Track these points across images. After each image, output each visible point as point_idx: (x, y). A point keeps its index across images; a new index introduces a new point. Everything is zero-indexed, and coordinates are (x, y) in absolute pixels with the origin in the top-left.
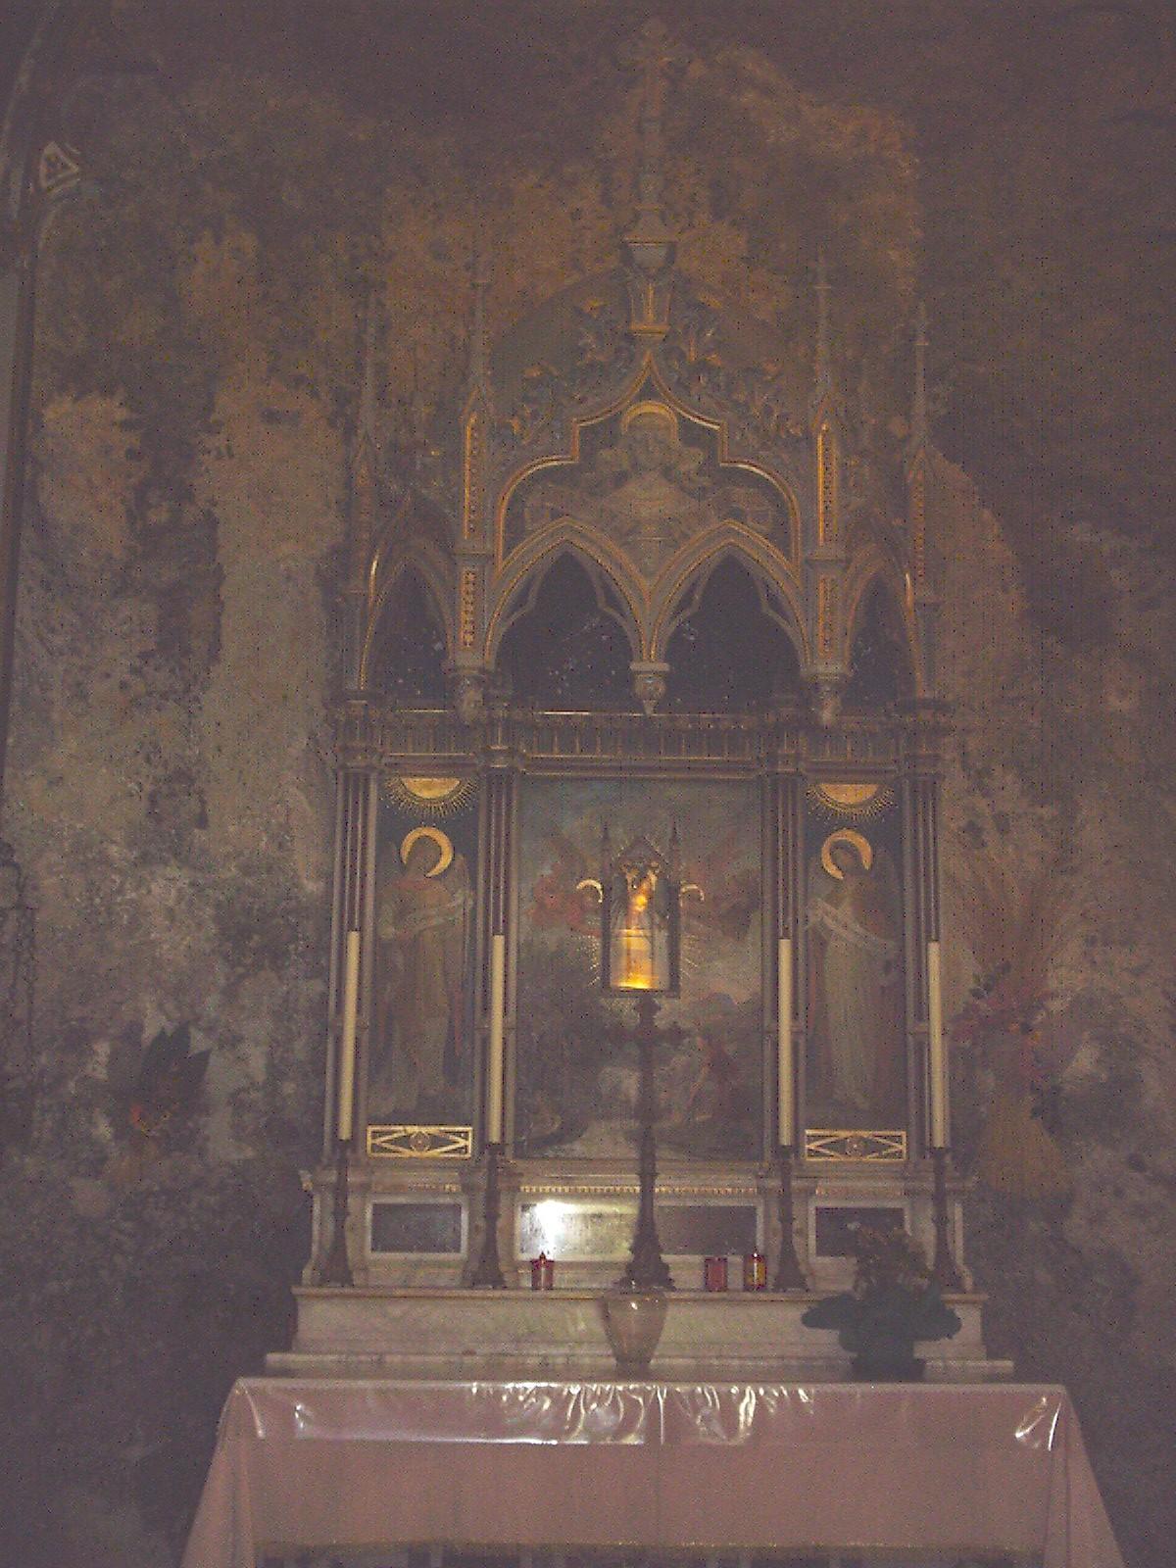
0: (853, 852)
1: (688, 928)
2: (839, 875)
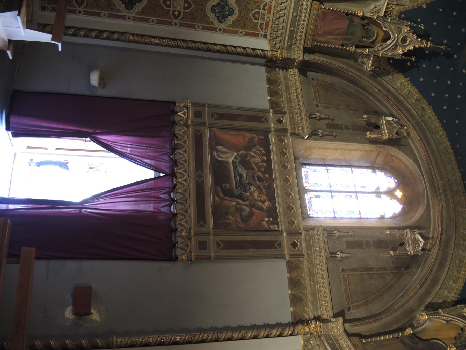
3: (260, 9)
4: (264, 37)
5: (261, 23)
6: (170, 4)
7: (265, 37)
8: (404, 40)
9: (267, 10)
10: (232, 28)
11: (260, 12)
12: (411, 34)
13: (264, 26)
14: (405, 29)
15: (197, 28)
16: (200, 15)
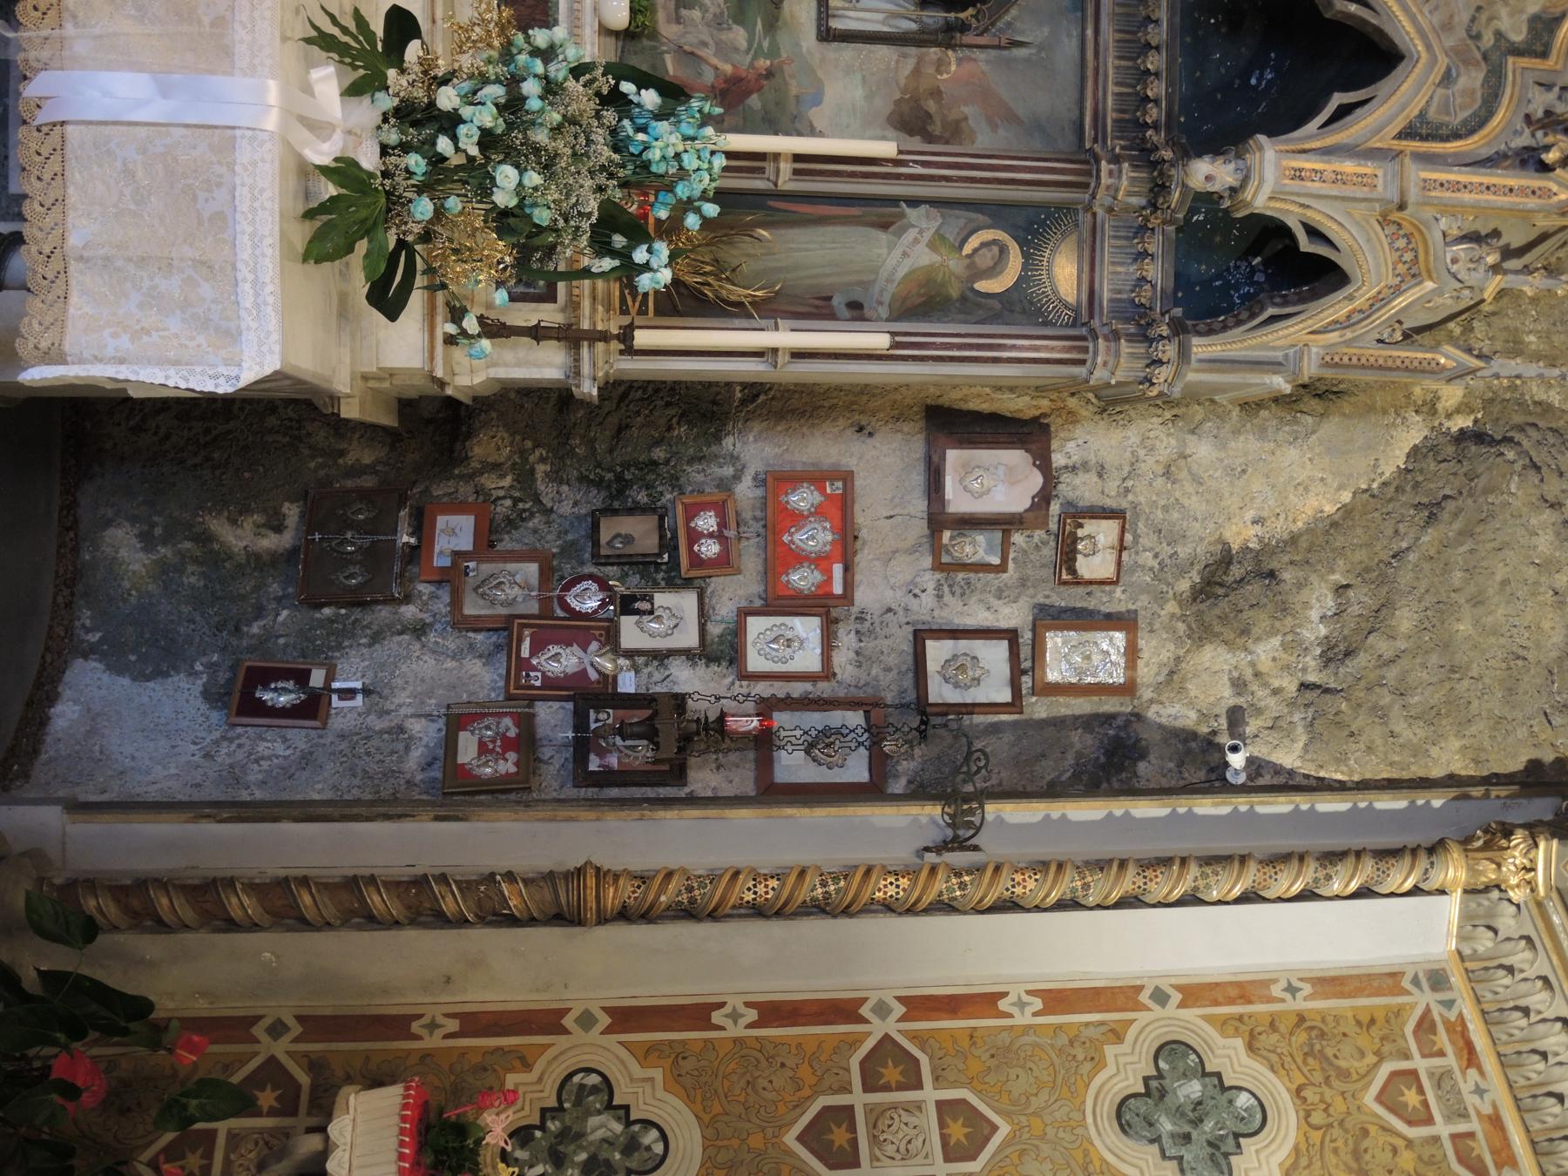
0: (993, 271)
1: (905, 56)
2: (967, 249)
3: (1407, 1056)
9: (1449, 1049)
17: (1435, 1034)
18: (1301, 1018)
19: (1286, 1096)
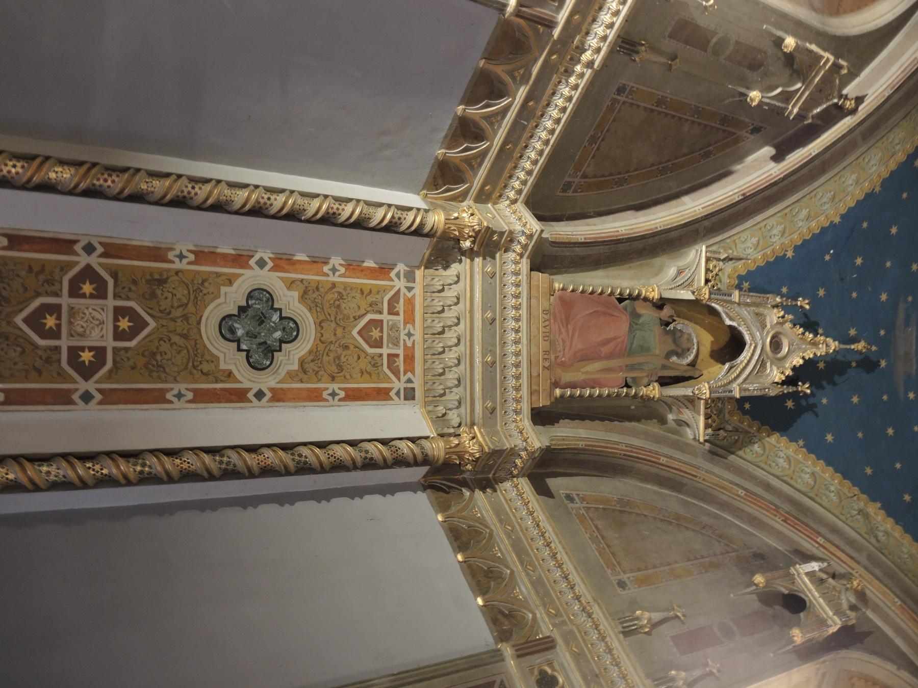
3: (381, 313)
4: (406, 399)
5: (390, 356)
6: (59, 326)
7: (409, 395)
8: (776, 344)
9: (402, 313)
10: (301, 381)
11: (382, 321)
12: (788, 325)
13: (400, 362)
14: (773, 316)
15: (175, 400)
16: (179, 352)
17: (398, 304)
18: (334, 285)
19: (313, 326)
